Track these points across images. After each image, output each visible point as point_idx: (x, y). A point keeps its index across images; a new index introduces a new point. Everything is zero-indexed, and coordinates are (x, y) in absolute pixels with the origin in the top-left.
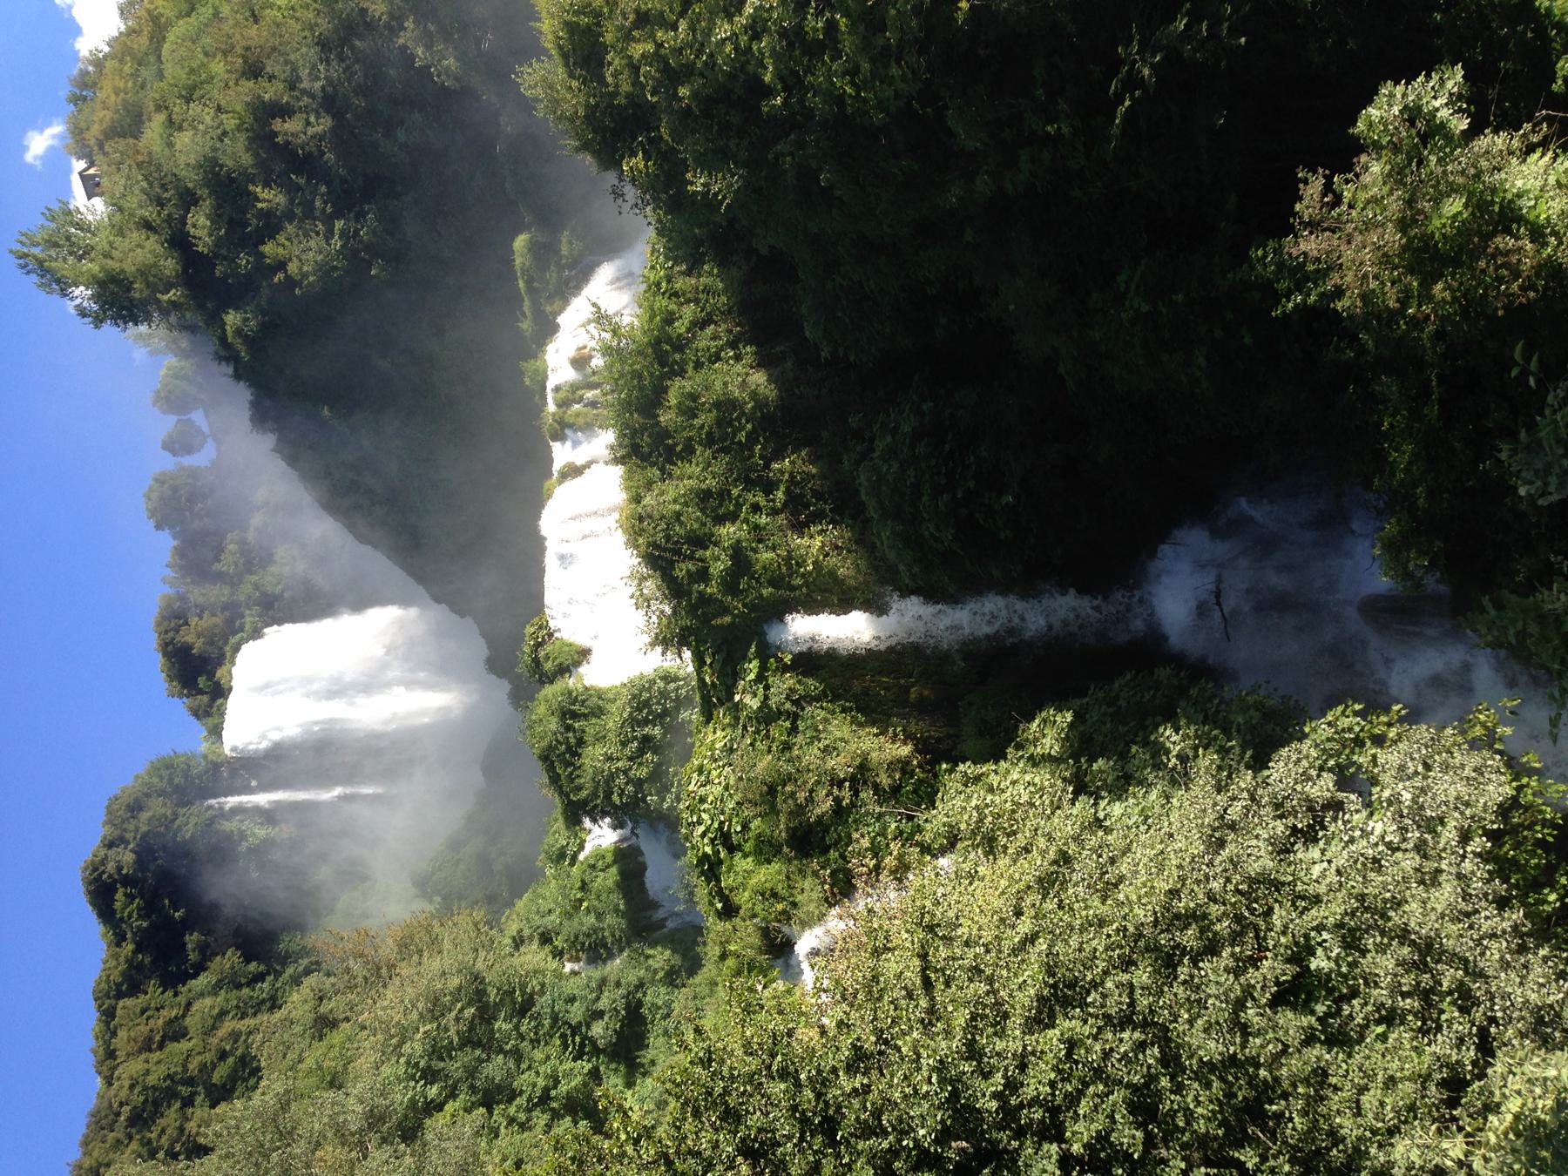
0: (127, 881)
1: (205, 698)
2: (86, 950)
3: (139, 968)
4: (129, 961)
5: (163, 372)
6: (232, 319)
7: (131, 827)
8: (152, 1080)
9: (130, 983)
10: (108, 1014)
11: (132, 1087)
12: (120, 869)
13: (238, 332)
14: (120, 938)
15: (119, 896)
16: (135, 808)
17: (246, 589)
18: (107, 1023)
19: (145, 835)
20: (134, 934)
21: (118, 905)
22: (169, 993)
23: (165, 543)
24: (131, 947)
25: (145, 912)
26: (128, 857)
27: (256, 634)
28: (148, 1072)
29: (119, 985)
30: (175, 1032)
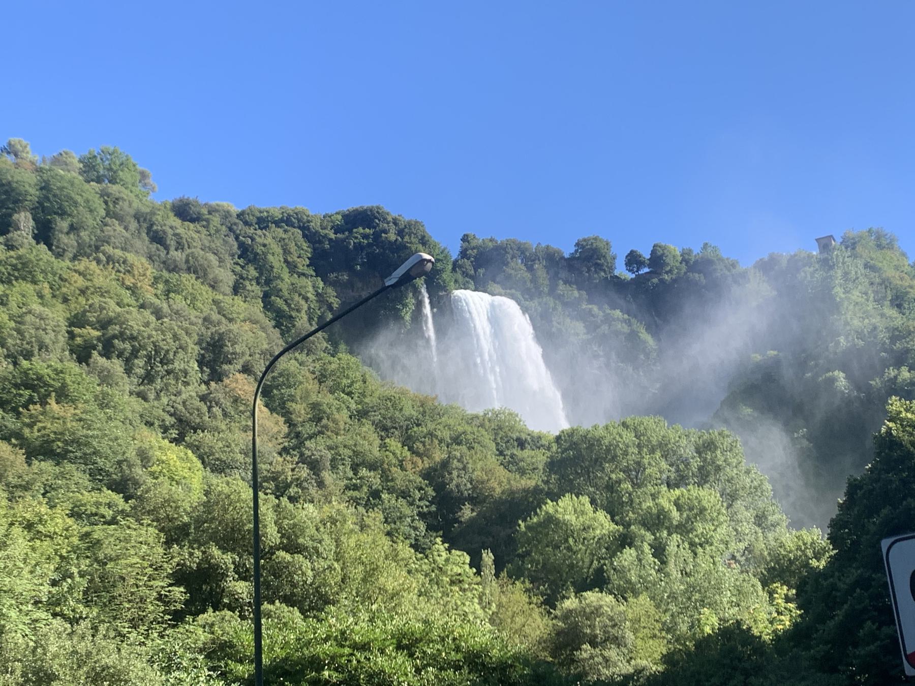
0: (377, 236)
1: (472, 272)
2: (324, 204)
3: (320, 242)
4: (325, 236)
5: (672, 247)
6: (841, 375)
7: (413, 240)
8: (270, 257)
9: (310, 236)
10: (286, 221)
11: (265, 245)
12: (385, 232)
13: (833, 380)
14: (337, 229)
15: (367, 230)
16: (424, 241)
17: (550, 301)
18: (282, 220)
19: (406, 248)
20: (343, 240)
21: (361, 230)
22: (308, 262)
23: (568, 250)
24: (333, 236)
25: (359, 247)
26: (392, 236)
27: (525, 310)
28: (273, 254)
29: (308, 228)
30: (292, 267)
